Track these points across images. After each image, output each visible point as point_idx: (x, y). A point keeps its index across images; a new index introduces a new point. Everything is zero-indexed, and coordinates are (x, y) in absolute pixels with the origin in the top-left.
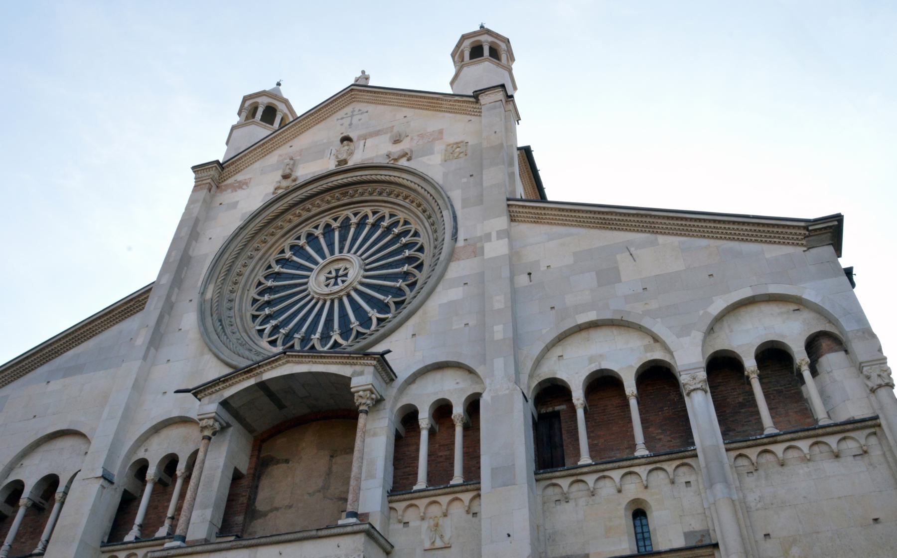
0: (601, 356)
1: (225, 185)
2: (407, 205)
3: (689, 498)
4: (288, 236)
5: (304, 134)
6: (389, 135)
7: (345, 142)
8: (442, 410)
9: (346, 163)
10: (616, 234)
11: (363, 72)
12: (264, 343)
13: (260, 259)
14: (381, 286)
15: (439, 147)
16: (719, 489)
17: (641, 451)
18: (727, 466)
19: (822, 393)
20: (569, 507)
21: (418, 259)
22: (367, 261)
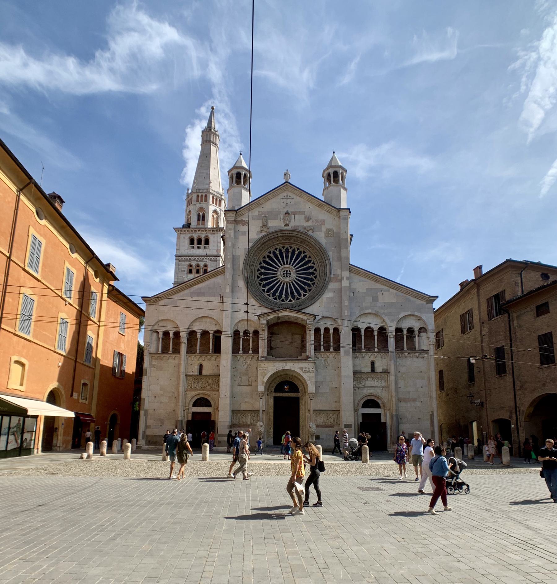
2: (311, 251)
3: (385, 361)
6: (304, 216)
7: (287, 215)
8: (327, 330)
10: (379, 285)
11: (287, 170)
12: (266, 295)
15: (324, 229)
16: (392, 361)
17: (376, 349)
18: (395, 356)
19: (419, 341)
20: (358, 359)
21: (314, 274)
22: (297, 270)
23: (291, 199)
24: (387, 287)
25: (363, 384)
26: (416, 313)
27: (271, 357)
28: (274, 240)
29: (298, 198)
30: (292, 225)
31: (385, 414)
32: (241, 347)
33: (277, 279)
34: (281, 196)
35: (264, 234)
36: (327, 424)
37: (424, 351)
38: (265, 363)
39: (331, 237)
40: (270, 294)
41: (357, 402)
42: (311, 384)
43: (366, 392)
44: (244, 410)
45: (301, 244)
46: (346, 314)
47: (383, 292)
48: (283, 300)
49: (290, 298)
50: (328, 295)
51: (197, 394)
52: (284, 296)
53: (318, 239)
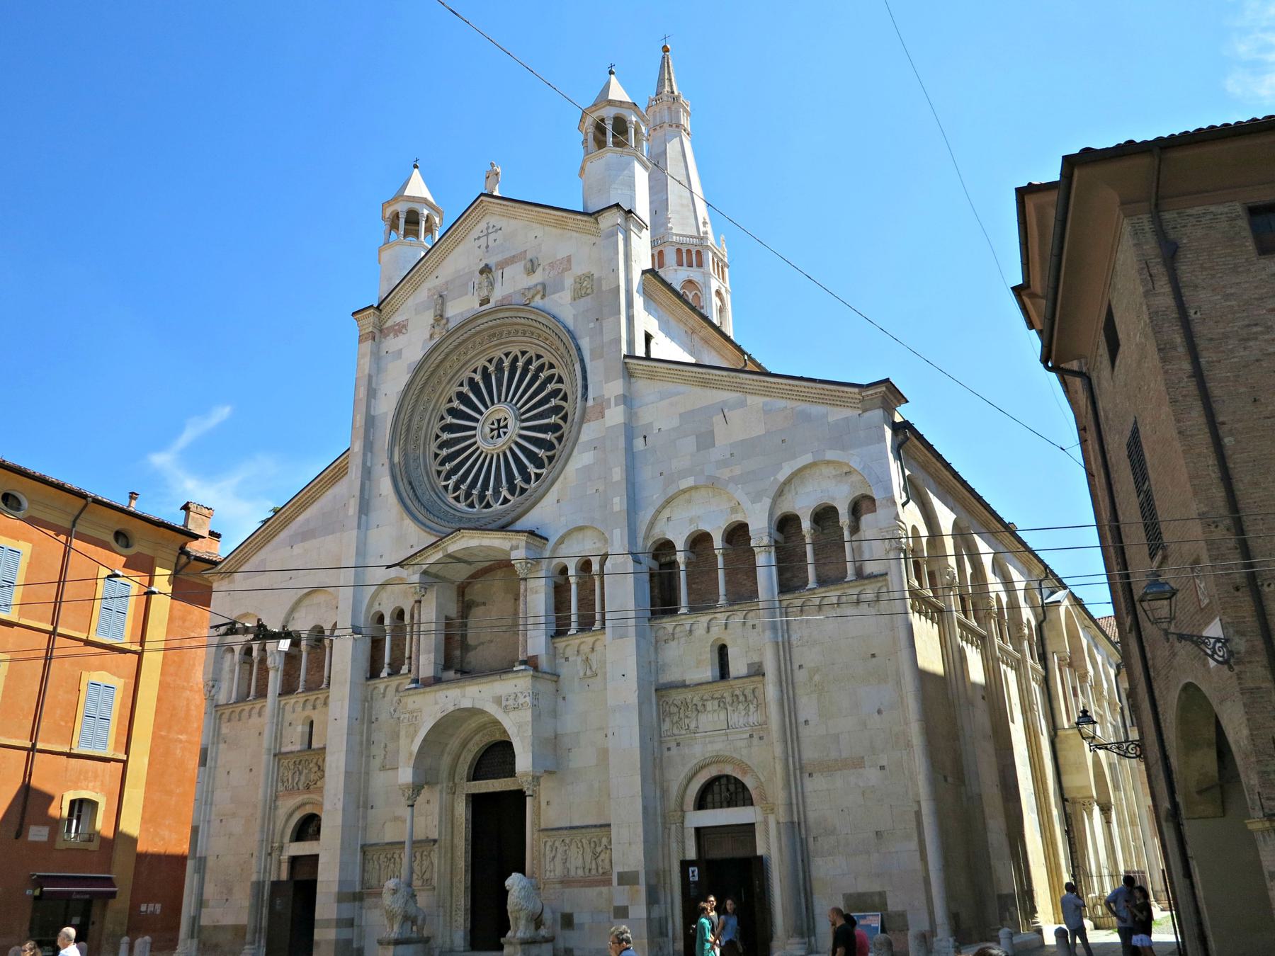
0: (699, 517)
1: (387, 328)
2: (549, 348)
4: (452, 383)
5: (447, 259)
9: (489, 302)
10: (714, 391)
11: (492, 165)
12: (450, 498)
13: (433, 410)
14: (537, 439)
20: (673, 644)
23: (496, 231)
24: (739, 394)
25: (693, 726)
26: (830, 455)
27: (451, 674)
28: (462, 349)
29: (512, 221)
30: (497, 295)
31: (766, 823)
32: (387, 660)
33: (478, 448)
34: (476, 232)
35: (437, 338)
36: (594, 872)
37: (876, 576)
38: (415, 698)
39: (588, 294)
40: (459, 495)
41: (674, 789)
42: (524, 747)
43: (698, 751)
44: (387, 844)
45: (525, 339)
46: (617, 508)
47: (726, 411)
48: (488, 506)
49: (504, 493)
50: (580, 461)
51: (298, 804)
52: (489, 493)
53: (555, 311)
